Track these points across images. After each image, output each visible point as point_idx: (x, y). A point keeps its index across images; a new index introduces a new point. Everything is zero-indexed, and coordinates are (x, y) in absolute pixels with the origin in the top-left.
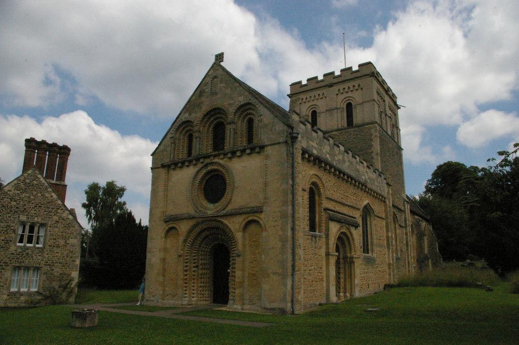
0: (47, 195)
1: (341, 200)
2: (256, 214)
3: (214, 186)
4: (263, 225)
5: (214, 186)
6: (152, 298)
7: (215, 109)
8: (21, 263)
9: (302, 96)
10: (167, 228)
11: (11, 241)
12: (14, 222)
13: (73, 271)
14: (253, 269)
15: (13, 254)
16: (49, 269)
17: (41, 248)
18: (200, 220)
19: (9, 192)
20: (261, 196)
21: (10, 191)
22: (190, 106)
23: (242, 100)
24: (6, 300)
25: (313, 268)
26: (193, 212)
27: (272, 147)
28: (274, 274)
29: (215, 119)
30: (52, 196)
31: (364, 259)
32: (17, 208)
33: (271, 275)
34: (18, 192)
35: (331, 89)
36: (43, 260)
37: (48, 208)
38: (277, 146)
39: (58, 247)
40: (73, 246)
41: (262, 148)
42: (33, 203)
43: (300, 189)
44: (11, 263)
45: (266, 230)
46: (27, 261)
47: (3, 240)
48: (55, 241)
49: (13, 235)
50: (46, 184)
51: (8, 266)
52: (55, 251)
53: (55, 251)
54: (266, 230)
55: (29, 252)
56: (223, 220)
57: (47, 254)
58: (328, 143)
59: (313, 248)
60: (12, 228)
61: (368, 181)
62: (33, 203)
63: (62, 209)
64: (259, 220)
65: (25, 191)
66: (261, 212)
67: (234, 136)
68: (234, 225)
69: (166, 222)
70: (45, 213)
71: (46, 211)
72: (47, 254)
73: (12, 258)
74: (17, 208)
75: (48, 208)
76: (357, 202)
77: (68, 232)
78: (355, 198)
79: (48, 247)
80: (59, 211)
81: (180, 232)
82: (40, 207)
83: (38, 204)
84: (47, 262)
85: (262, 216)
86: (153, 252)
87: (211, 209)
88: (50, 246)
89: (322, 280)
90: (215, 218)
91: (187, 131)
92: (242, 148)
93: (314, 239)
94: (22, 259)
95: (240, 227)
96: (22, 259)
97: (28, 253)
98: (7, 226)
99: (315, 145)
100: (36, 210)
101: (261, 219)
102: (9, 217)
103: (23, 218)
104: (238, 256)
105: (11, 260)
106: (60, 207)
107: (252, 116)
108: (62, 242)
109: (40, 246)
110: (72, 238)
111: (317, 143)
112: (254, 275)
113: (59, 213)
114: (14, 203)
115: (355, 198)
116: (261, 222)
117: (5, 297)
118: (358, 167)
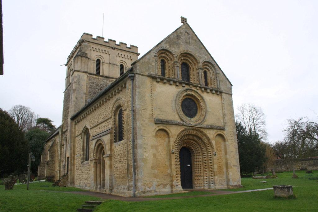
2: (223, 131)
3: (190, 106)
4: (226, 138)
5: (190, 106)
6: (148, 189)
7: (191, 55)
9: (92, 45)
10: (157, 129)
14: (220, 163)
18: (187, 127)
20: (222, 121)
22: (168, 40)
23: (206, 58)
26: (179, 121)
27: (226, 94)
28: (234, 166)
29: (184, 59)
33: (233, 167)
35: (113, 50)
38: (228, 95)
41: (221, 93)
45: (228, 141)
54: (228, 141)
56: (203, 131)
64: (224, 135)
66: (225, 130)
67: (196, 76)
68: (211, 134)
69: (156, 123)
81: (170, 135)
85: (225, 132)
86: (145, 148)
87: (193, 121)
90: (198, 128)
91: (162, 57)
92: (211, 88)
95: (213, 137)
101: (225, 134)
104: (215, 155)
107: (208, 71)
112: (220, 167)
116: (225, 136)
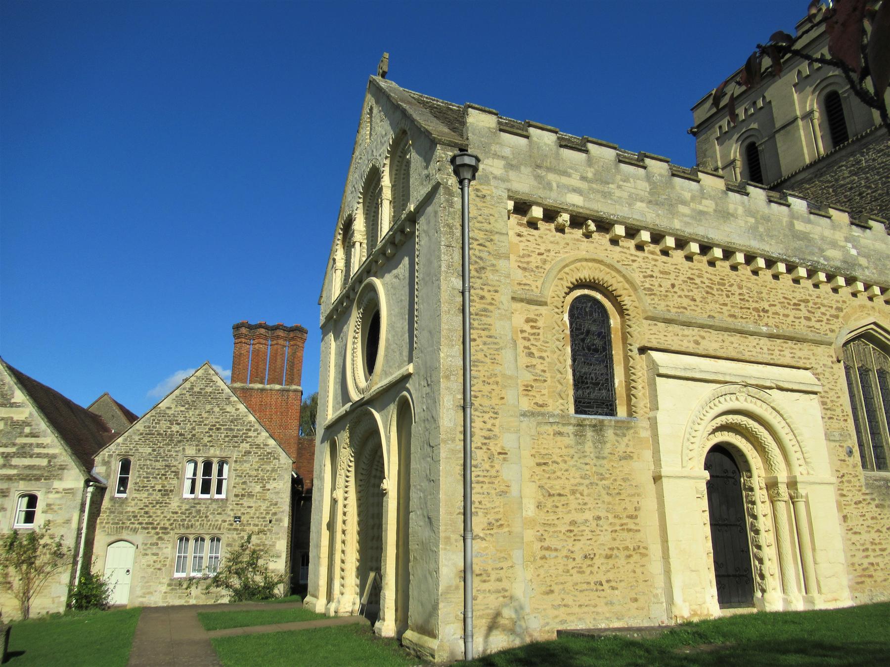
0: (229, 408)
1: (730, 322)
8: (188, 528)
11: (171, 491)
12: (176, 460)
13: (279, 539)
15: (176, 513)
16: (236, 537)
17: (222, 500)
19: (168, 411)
21: (169, 408)
24: (165, 593)
25: (588, 515)
30: (237, 409)
31: (868, 485)
32: (181, 435)
34: (183, 409)
36: (225, 521)
37: (231, 430)
39: (250, 495)
40: (278, 493)
42: (205, 425)
43: (504, 298)
44: (172, 529)
46: (198, 524)
47: (160, 491)
48: (244, 486)
49: (175, 482)
50: (227, 390)
51: (168, 533)
52: (246, 504)
53: (246, 504)
55: (203, 508)
57: (232, 510)
58: (641, 170)
59: (587, 460)
60: (173, 469)
61: (863, 261)
62: (205, 425)
63: (255, 430)
65: (192, 406)
70: (227, 439)
71: (228, 436)
72: (232, 510)
73: (175, 520)
74: (181, 435)
75: (231, 430)
76: (812, 323)
77: (268, 468)
78: (804, 312)
79: (234, 499)
80: (250, 434)
82: (218, 429)
83: (214, 426)
84: (231, 525)
88: (236, 496)
89: (640, 550)
93: (589, 433)
94: (190, 521)
96: (190, 521)
97: (200, 511)
98: (166, 466)
99: (575, 182)
100: (211, 436)
102: (169, 451)
103: (191, 451)
105: (171, 524)
106: (253, 426)
108: (258, 488)
109: (223, 496)
110: (275, 479)
111: (583, 178)
113: (250, 437)
114: (175, 428)
115: (804, 312)
117: (164, 588)
118: (799, 226)
